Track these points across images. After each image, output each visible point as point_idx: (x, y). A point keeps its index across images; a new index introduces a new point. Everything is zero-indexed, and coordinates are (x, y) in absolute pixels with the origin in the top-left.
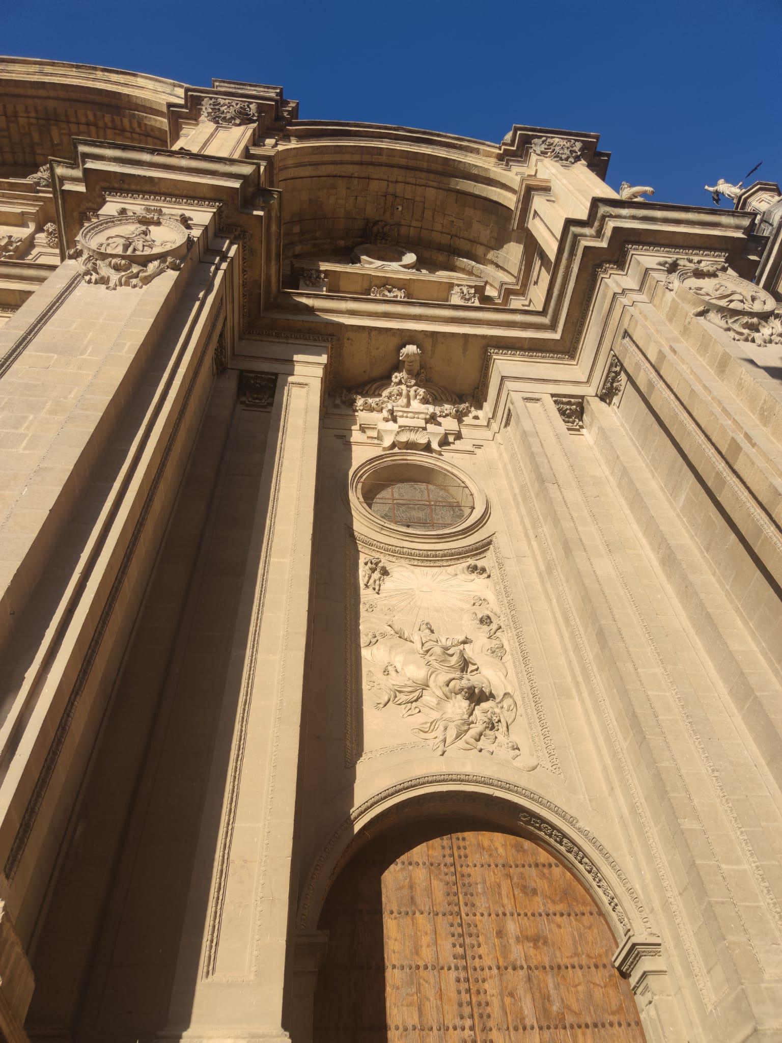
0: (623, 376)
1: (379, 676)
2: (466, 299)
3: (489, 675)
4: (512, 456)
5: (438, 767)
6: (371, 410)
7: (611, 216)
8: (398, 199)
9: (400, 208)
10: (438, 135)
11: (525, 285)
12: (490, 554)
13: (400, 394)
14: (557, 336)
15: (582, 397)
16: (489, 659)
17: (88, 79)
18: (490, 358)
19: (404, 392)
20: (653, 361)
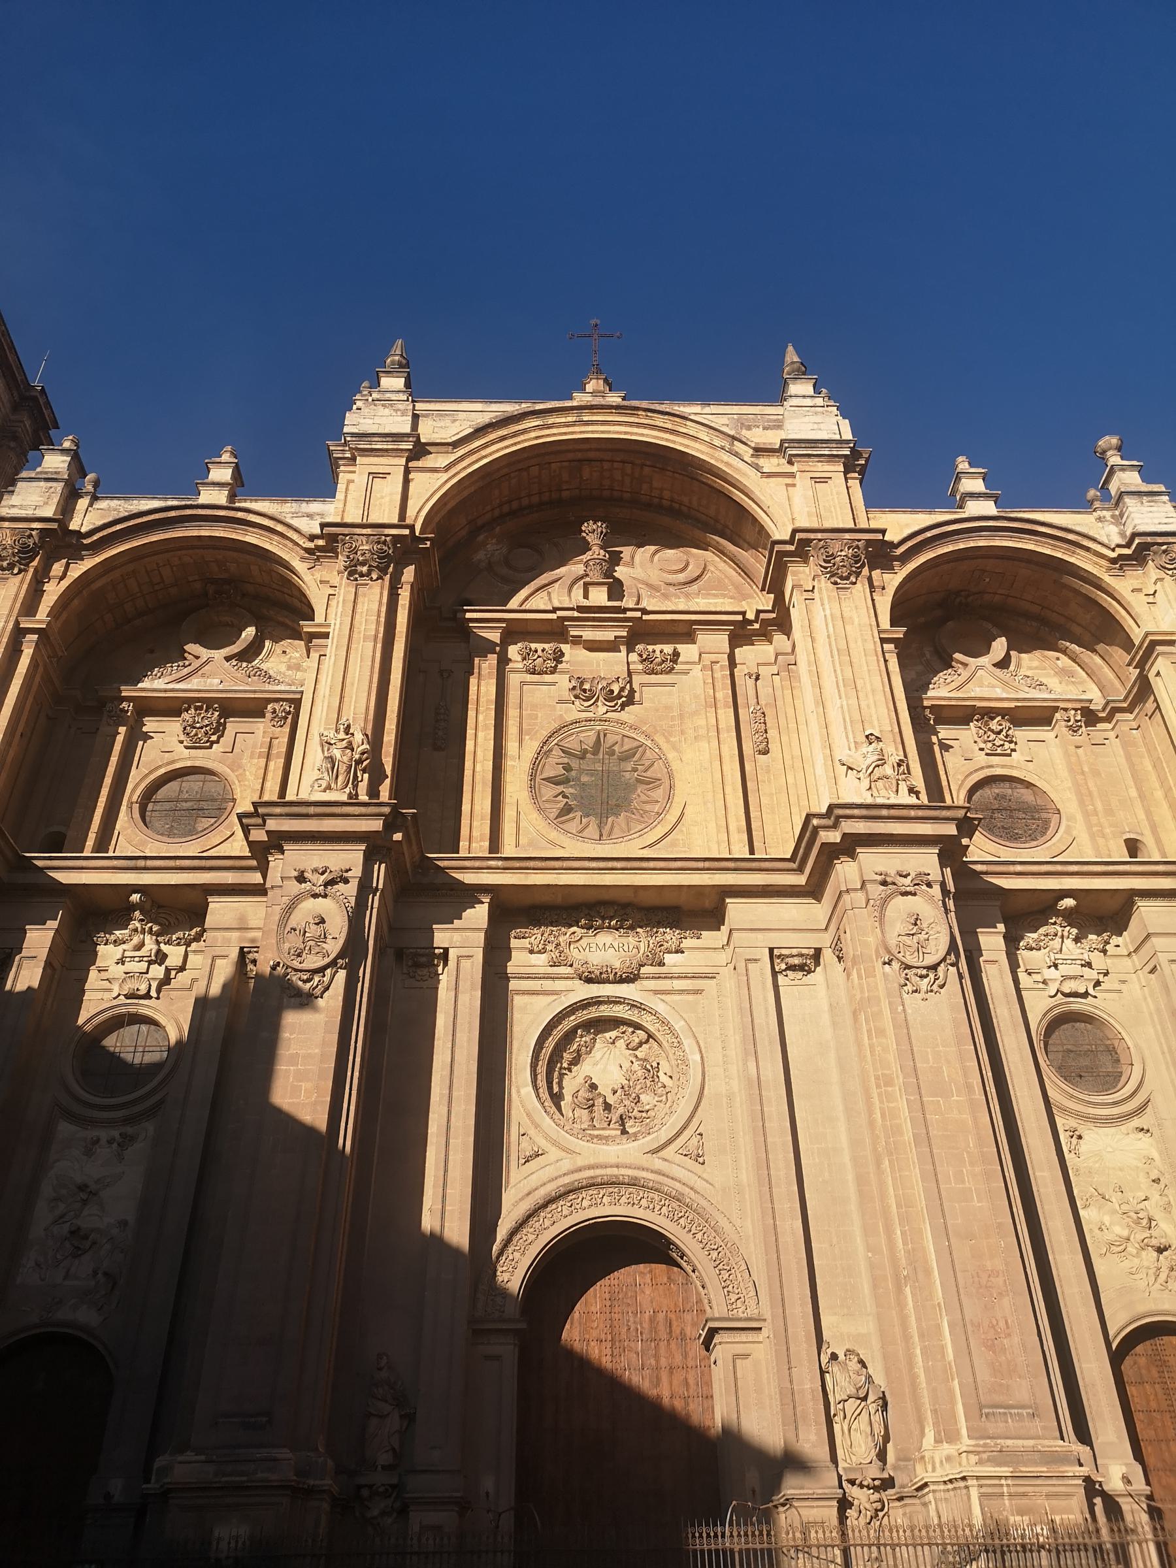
1: (1097, 1231)
3: (1167, 1230)
4: (1158, 1010)
5: (1150, 1306)
6: (1031, 949)
17: (631, 424)
18: (1133, 903)
19: (1060, 934)
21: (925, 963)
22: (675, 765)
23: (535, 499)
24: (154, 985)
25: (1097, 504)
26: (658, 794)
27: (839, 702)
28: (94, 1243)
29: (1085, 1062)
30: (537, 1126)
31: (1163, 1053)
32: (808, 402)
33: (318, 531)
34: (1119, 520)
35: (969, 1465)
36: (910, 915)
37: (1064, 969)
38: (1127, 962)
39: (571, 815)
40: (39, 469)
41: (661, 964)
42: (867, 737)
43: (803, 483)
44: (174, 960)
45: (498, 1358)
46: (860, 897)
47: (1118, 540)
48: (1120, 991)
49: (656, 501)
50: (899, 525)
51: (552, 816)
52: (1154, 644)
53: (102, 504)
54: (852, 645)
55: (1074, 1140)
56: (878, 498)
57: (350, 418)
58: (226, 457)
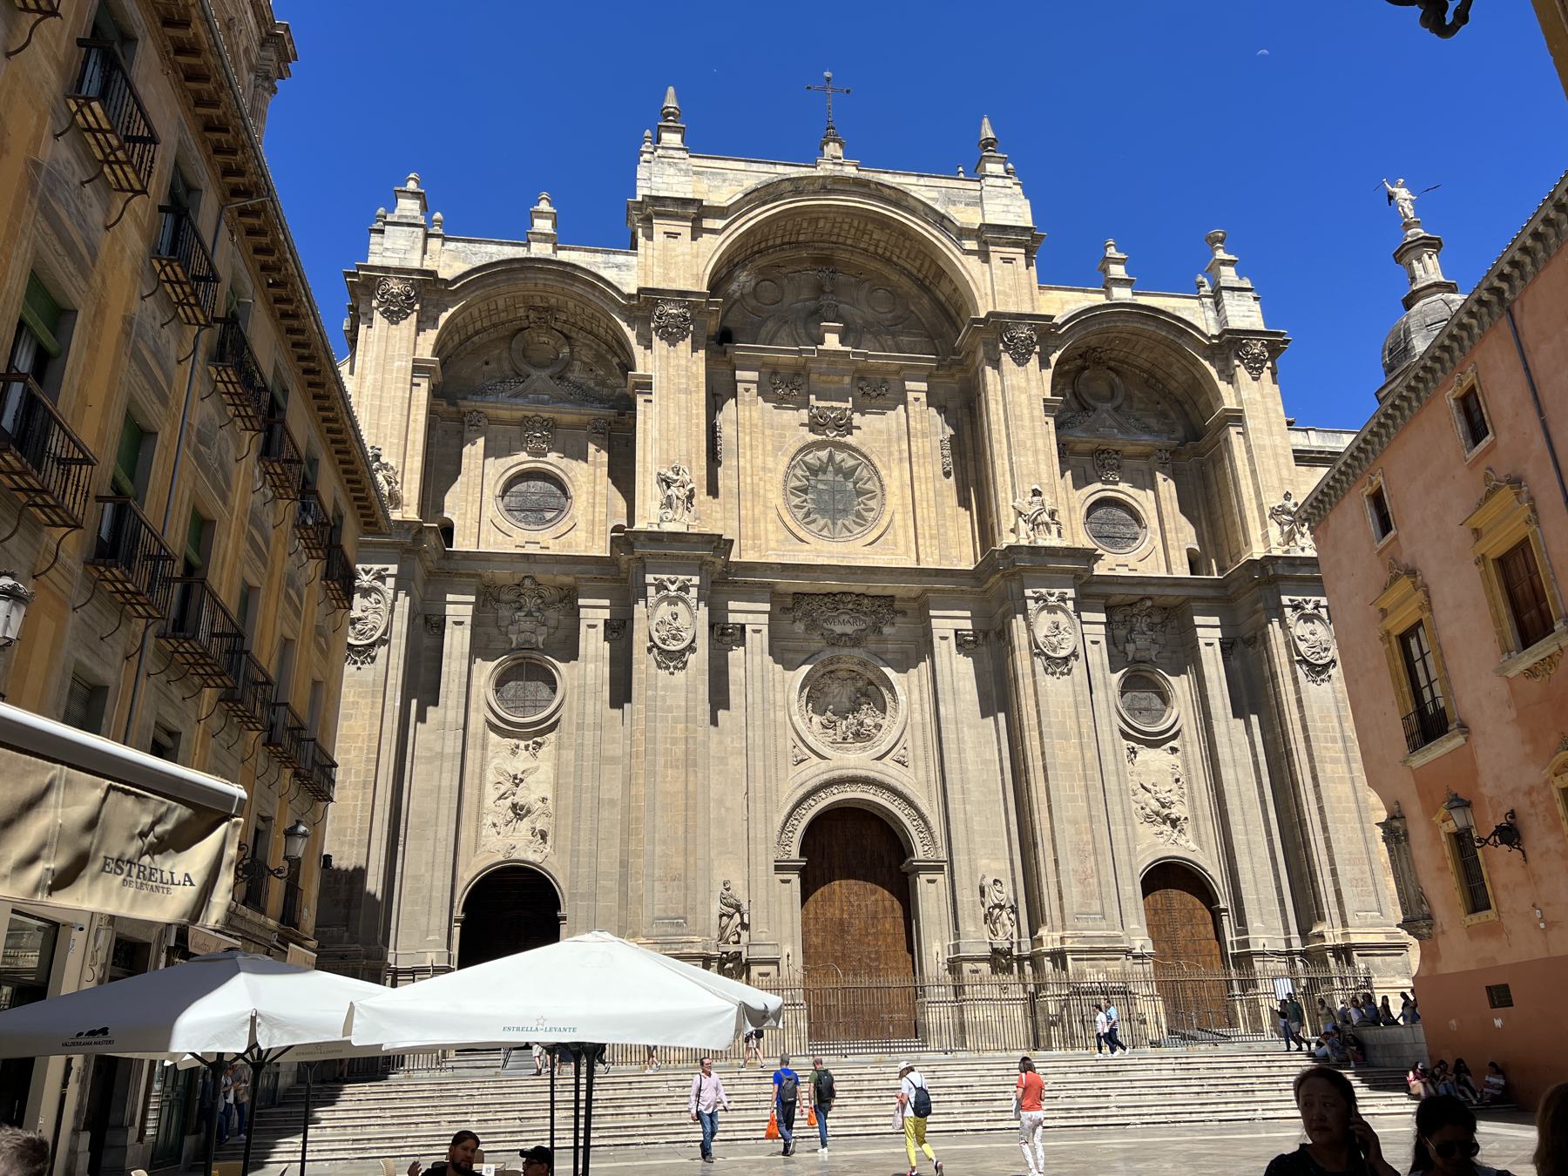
22: (886, 481)
23: (778, 241)
24: (541, 639)
25: (1202, 291)
26: (872, 504)
28: (529, 812)
30: (803, 741)
32: (999, 182)
33: (635, 291)
34: (1218, 304)
35: (1068, 944)
39: (813, 516)
40: (397, 212)
41: (880, 632)
43: (995, 258)
44: (552, 623)
45: (788, 881)
47: (1214, 330)
49: (872, 249)
50: (1063, 304)
51: (800, 515)
53: (451, 245)
54: (1025, 411)
56: (1050, 279)
57: (642, 172)
58: (544, 206)
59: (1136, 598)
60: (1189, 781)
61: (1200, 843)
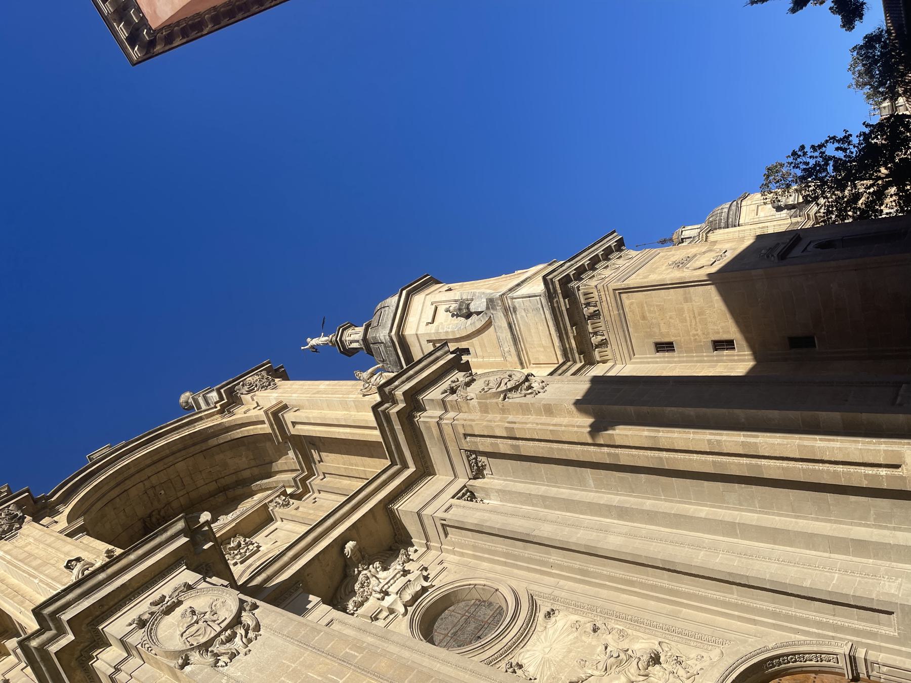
0: (479, 458)
2: (287, 505)
3: (642, 645)
4: (475, 548)
6: (361, 604)
7: (393, 390)
8: (157, 488)
9: (163, 492)
10: (161, 428)
11: (310, 469)
12: (539, 602)
13: (368, 578)
14: (412, 469)
15: (465, 486)
16: (627, 640)
19: (369, 575)
20: (505, 435)
21: (223, 625)
27: (36, 581)
29: (472, 626)
31: (505, 564)
36: (183, 615)
37: (393, 589)
38: (433, 553)
42: (67, 567)
46: (135, 661)
48: (444, 569)
52: (275, 414)
55: (519, 672)
59: (335, 550)
60: (607, 614)
61: (714, 642)
